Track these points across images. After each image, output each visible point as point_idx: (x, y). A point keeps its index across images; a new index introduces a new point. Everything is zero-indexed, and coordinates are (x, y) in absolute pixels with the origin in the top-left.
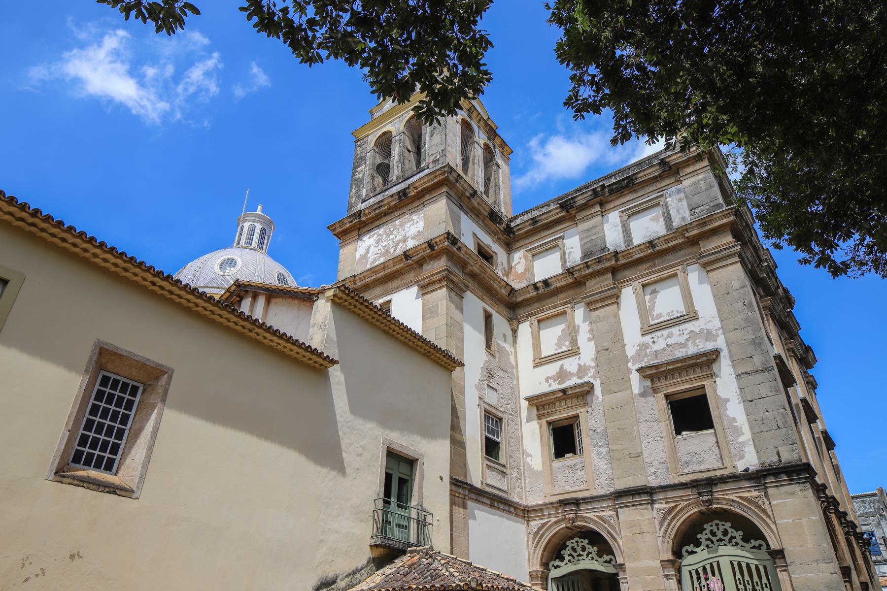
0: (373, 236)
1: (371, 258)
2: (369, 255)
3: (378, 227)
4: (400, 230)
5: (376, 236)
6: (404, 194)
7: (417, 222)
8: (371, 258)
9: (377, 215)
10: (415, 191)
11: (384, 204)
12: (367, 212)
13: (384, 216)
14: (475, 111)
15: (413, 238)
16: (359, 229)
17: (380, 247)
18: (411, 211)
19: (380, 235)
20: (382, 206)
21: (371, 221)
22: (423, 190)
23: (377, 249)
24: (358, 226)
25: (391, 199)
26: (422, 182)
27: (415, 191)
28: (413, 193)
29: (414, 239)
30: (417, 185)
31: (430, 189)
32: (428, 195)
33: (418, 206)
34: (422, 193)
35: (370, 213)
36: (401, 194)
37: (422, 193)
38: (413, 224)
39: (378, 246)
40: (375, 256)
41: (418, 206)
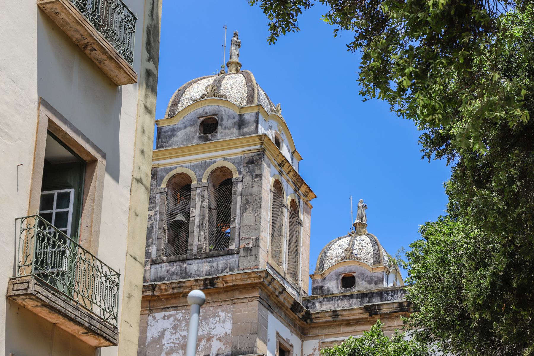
0: (169, 317)
1: (167, 346)
2: (164, 341)
3: (176, 308)
4: (203, 322)
5: (172, 319)
6: (210, 283)
7: (224, 321)
8: (167, 346)
9: (174, 294)
10: (225, 285)
11: (186, 286)
12: (163, 287)
13: (183, 296)
14: (286, 164)
15: (219, 339)
16: (150, 301)
17: (178, 336)
18: (216, 304)
19: (176, 319)
20: (182, 287)
21: (166, 297)
22: (233, 286)
23: (174, 337)
24: (150, 298)
25: (194, 283)
26: (234, 278)
27: (225, 285)
28: (221, 286)
29: (221, 341)
30: (228, 279)
31: (241, 287)
32: (238, 292)
33: (226, 301)
34: (232, 288)
35: (166, 290)
36: (207, 282)
37: (232, 288)
38: (219, 321)
39: (175, 333)
40: (172, 345)
41: (226, 301)
